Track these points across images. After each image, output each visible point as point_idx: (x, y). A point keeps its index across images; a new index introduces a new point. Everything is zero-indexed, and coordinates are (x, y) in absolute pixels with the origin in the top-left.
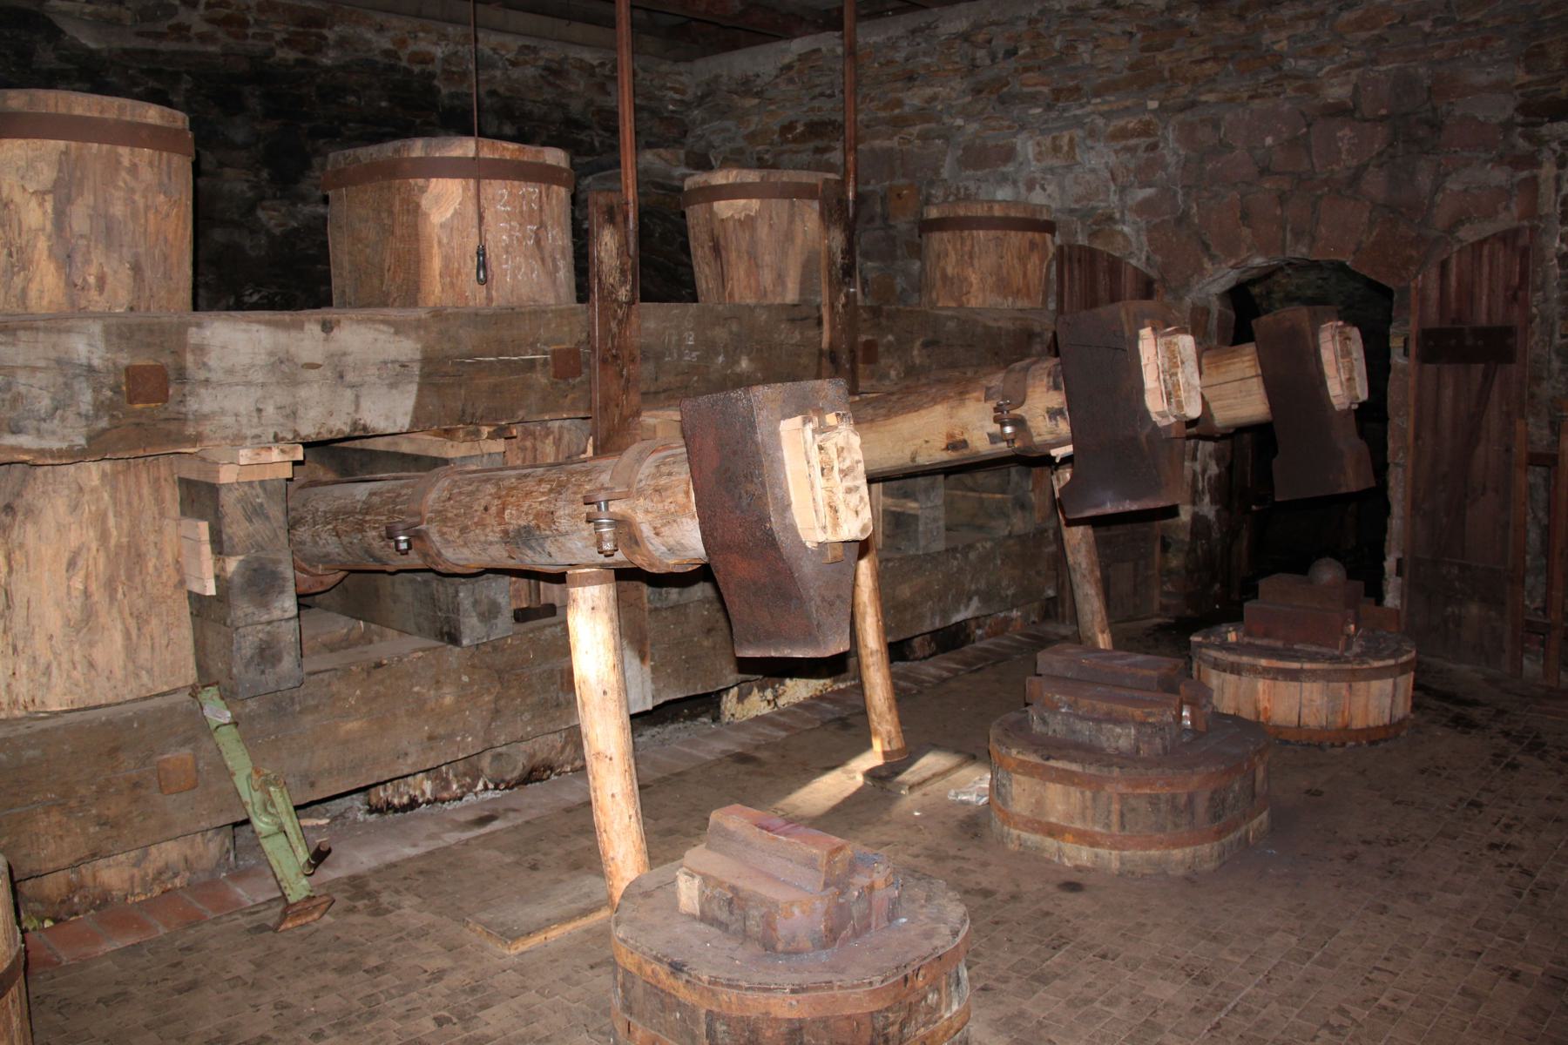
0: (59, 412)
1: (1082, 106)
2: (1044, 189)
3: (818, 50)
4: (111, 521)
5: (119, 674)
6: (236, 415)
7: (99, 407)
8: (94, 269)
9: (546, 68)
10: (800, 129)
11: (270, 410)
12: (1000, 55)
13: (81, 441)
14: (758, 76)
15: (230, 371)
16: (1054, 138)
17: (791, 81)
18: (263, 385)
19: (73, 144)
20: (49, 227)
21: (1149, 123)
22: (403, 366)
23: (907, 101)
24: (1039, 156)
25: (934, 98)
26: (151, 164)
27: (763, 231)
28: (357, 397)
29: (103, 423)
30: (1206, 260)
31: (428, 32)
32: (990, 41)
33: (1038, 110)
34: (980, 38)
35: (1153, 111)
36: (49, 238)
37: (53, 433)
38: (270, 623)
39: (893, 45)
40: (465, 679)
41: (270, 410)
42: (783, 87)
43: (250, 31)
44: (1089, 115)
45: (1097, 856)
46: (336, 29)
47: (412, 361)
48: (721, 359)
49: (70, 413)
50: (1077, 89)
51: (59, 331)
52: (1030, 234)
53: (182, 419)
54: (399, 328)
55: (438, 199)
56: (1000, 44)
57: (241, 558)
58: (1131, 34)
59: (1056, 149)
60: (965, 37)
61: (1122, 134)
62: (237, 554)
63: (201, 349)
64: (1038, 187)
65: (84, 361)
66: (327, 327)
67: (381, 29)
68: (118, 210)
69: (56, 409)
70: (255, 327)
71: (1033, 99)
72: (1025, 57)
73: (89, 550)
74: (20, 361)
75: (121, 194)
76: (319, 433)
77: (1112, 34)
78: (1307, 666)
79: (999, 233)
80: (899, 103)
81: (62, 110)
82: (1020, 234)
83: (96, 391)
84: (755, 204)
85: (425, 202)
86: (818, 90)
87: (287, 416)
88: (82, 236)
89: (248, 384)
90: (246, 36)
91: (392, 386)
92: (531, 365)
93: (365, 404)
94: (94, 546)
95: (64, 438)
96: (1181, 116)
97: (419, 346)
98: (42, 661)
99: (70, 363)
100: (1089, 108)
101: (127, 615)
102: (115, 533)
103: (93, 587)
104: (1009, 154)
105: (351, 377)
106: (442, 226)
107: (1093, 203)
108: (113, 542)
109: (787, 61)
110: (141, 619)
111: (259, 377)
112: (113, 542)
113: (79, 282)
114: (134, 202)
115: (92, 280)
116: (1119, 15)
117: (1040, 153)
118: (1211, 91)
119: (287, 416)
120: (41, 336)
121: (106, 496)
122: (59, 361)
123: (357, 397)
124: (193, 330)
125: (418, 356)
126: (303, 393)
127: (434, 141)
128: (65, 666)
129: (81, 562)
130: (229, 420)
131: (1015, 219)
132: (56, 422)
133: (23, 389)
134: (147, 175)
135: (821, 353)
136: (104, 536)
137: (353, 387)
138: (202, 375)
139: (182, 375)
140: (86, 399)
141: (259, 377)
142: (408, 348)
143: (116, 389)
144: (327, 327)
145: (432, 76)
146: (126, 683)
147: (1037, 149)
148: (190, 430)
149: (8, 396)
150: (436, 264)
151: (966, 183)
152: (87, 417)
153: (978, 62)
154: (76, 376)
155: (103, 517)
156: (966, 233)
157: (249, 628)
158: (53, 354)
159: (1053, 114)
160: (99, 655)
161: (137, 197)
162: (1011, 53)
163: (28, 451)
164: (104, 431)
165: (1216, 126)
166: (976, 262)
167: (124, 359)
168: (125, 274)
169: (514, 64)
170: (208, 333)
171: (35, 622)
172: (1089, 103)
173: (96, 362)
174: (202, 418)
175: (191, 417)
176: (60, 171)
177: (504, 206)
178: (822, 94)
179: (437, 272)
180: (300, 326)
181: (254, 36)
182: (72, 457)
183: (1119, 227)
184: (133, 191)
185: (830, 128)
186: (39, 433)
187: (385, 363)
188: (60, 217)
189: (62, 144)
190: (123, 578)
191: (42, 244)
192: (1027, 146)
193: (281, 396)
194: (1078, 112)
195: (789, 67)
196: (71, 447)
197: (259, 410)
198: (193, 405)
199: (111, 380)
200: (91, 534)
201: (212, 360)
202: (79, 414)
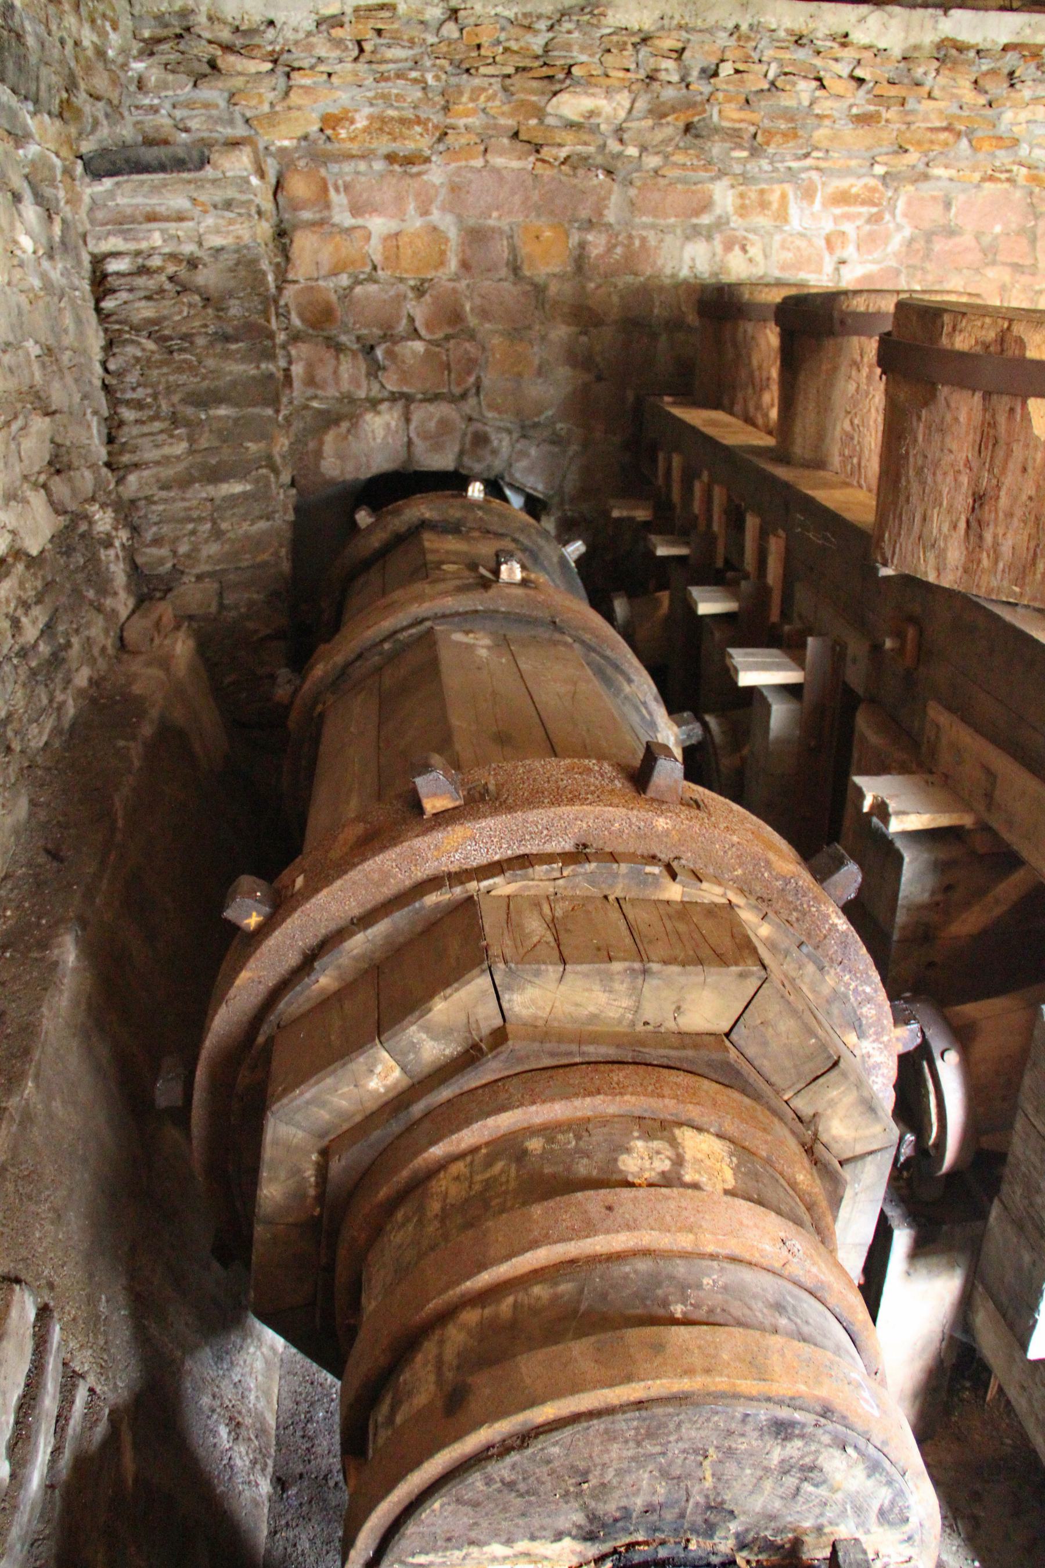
1: (798, 158)
2: (744, 249)
10: (361, 123)
12: (695, 73)
14: (271, 23)
17: (338, 43)
21: (874, 190)
23: (549, 109)
24: (743, 210)
25: (591, 114)
34: (669, 43)
56: (696, 59)
58: (861, 81)
61: (843, 198)
64: (737, 248)
80: (540, 113)
96: (910, 188)
100: (808, 162)
104: (706, 205)
117: (743, 206)
118: (946, 167)
147: (739, 202)
151: (644, 233)
153: (663, 76)
159: (765, 164)
165: (948, 205)
172: (807, 156)
185: (418, 129)
195: (336, 21)
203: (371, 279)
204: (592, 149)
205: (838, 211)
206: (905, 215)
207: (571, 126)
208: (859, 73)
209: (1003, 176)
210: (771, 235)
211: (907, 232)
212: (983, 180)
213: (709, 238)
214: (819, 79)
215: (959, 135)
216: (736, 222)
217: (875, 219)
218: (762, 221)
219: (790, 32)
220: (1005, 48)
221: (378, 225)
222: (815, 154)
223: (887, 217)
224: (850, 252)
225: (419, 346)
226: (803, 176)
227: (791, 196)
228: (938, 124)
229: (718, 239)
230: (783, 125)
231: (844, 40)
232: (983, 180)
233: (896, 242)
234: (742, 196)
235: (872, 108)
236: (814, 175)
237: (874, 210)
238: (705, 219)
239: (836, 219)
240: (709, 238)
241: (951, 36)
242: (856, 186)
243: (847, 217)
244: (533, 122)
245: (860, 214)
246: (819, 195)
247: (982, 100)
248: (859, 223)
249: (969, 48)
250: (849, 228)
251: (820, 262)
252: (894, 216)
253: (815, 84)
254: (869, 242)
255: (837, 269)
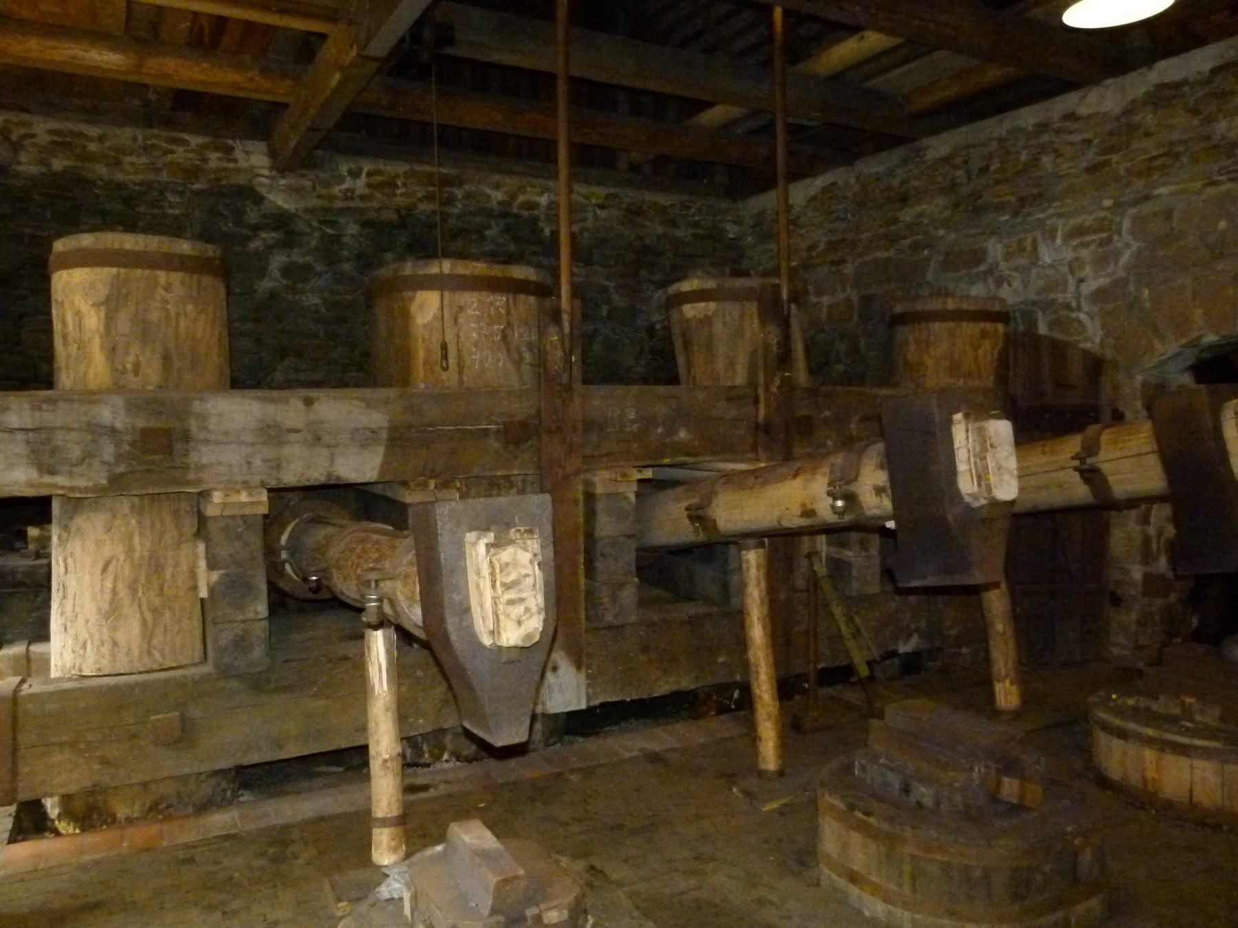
0: (87, 461)
1: (1044, 211)
2: (1010, 285)
3: (834, 184)
4: (137, 540)
5: (136, 652)
6: (230, 466)
7: (119, 458)
8: (131, 358)
9: (628, 210)
10: (822, 247)
11: (257, 462)
13: (104, 482)
15: (226, 433)
16: (1020, 241)
17: (815, 209)
18: (253, 444)
19: (123, 270)
20: (102, 329)
21: (1105, 218)
22: (373, 431)
23: (902, 219)
24: (1008, 256)
25: (921, 215)
26: (183, 284)
27: (718, 328)
28: (332, 454)
29: (121, 469)
30: (1156, 340)
31: (533, 186)
32: (966, 162)
33: (1006, 217)
34: (959, 160)
35: (1109, 208)
36: (101, 338)
37: (82, 475)
38: (244, 621)
39: (890, 172)
40: (419, 673)
41: (257, 462)
42: (810, 214)
43: (399, 192)
44: (1049, 217)
45: (890, 913)
46: (466, 187)
47: (381, 428)
48: (660, 430)
49: (96, 463)
50: (1040, 195)
51: (91, 402)
52: (982, 325)
53: (186, 468)
54: (369, 404)
55: (421, 307)
56: (976, 164)
57: (222, 572)
59: (1022, 250)
60: (947, 160)
61: (1080, 231)
62: (220, 568)
63: (203, 417)
64: (1005, 284)
65: (109, 424)
66: (308, 402)
67: (497, 186)
68: (154, 316)
69: (85, 458)
70: (247, 401)
71: (999, 208)
72: (995, 172)
73: (118, 560)
74: (59, 423)
75: (158, 305)
76: (299, 481)
77: (1071, 144)
78: (1198, 742)
79: (952, 325)
80: (895, 220)
81: (116, 246)
82: (971, 324)
83: (117, 446)
84: (712, 306)
85: (413, 308)
86: (835, 215)
87: (272, 468)
88: (123, 335)
89: (240, 443)
90: (395, 195)
91: (363, 446)
92: (486, 433)
93: (339, 460)
94: (122, 558)
95: (89, 479)
97: (387, 417)
98: (81, 639)
99: (97, 425)
100: (1050, 211)
101: (144, 607)
102: (138, 548)
103: (120, 587)
105: (327, 438)
106: (425, 326)
107: (1052, 296)
108: (137, 555)
109: (812, 193)
110: (156, 612)
111: (249, 438)
112: (137, 555)
113: (120, 367)
114: (167, 310)
115: (129, 366)
116: (1077, 125)
117: (1008, 253)
119: (272, 468)
120: (76, 406)
121: (133, 522)
122: (89, 424)
123: (332, 454)
124: (196, 403)
125: (386, 425)
126: (286, 451)
127: (421, 263)
128: (96, 643)
129: (111, 568)
130: (222, 469)
131: (967, 312)
132: (84, 466)
133: (60, 443)
134: (178, 290)
135: (757, 426)
136: (130, 551)
137: (329, 446)
138: (202, 436)
139: (186, 436)
140: (108, 451)
141: (249, 438)
142: (378, 419)
143: (133, 444)
144: (308, 402)
145: (536, 219)
146: (140, 658)
148: (192, 476)
149: (48, 448)
150: (421, 354)
152: (108, 464)
153: (958, 181)
154: (101, 435)
155: (131, 537)
156: (923, 325)
157: (226, 626)
158: (84, 418)
159: (1019, 220)
160: (121, 636)
161: (170, 307)
162: (984, 170)
163: (62, 488)
164: (122, 475)
165: (1168, 215)
166: (931, 349)
167: (141, 423)
168: (157, 363)
169: (602, 207)
170: (209, 405)
171: (78, 609)
172: (1049, 207)
173: (118, 425)
174: (201, 467)
175: (193, 466)
176: (111, 290)
177: (474, 310)
178: (838, 218)
179: (421, 362)
180: (285, 401)
181: (402, 195)
182: (96, 493)
183: (1074, 315)
184: (167, 302)
186: (71, 475)
187: (357, 429)
188: (109, 321)
189: (114, 270)
190: (143, 581)
191: (97, 342)
192: (995, 249)
193: (268, 452)
194: (1040, 216)
195: (814, 198)
196: (96, 485)
197: (249, 463)
198: (194, 458)
199: (129, 438)
200: (120, 549)
201: (212, 423)
202: (104, 463)
203: (823, 331)
204: (920, 237)
205: (1075, 243)
206: (1132, 232)
207: (909, 226)
208: (1086, 136)
209: (1223, 178)
210: (1029, 270)
211: (1135, 246)
212: (1205, 186)
213: (985, 280)
214: (1056, 151)
215: (1177, 156)
216: (1003, 265)
217: (1109, 240)
218: (1022, 261)
219: (1035, 125)
220: (1215, 71)
221: (825, 300)
222: (1054, 205)
223: (1116, 238)
224: (1088, 270)
225: (841, 368)
226: (1049, 222)
227: (1039, 237)
228: (1155, 153)
229: (991, 280)
230: (1035, 191)
231: (1071, 116)
232: (1205, 186)
233: (1125, 259)
234: (1007, 247)
235: (1102, 158)
236: (1055, 219)
237: (1104, 235)
238: (982, 268)
239: (1075, 248)
240: (985, 280)
241: (1159, 81)
242: (1087, 220)
243: (1084, 245)
244: (893, 228)
245: (1093, 241)
246: (1059, 233)
247: (1196, 122)
248: (1092, 247)
249: (1184, 82)
250: (1085, 253)
251: (1066, 282)
252: (1120, 233)
253: (1052, 156)
254: (1101, 262)
255: (1078, 287)
